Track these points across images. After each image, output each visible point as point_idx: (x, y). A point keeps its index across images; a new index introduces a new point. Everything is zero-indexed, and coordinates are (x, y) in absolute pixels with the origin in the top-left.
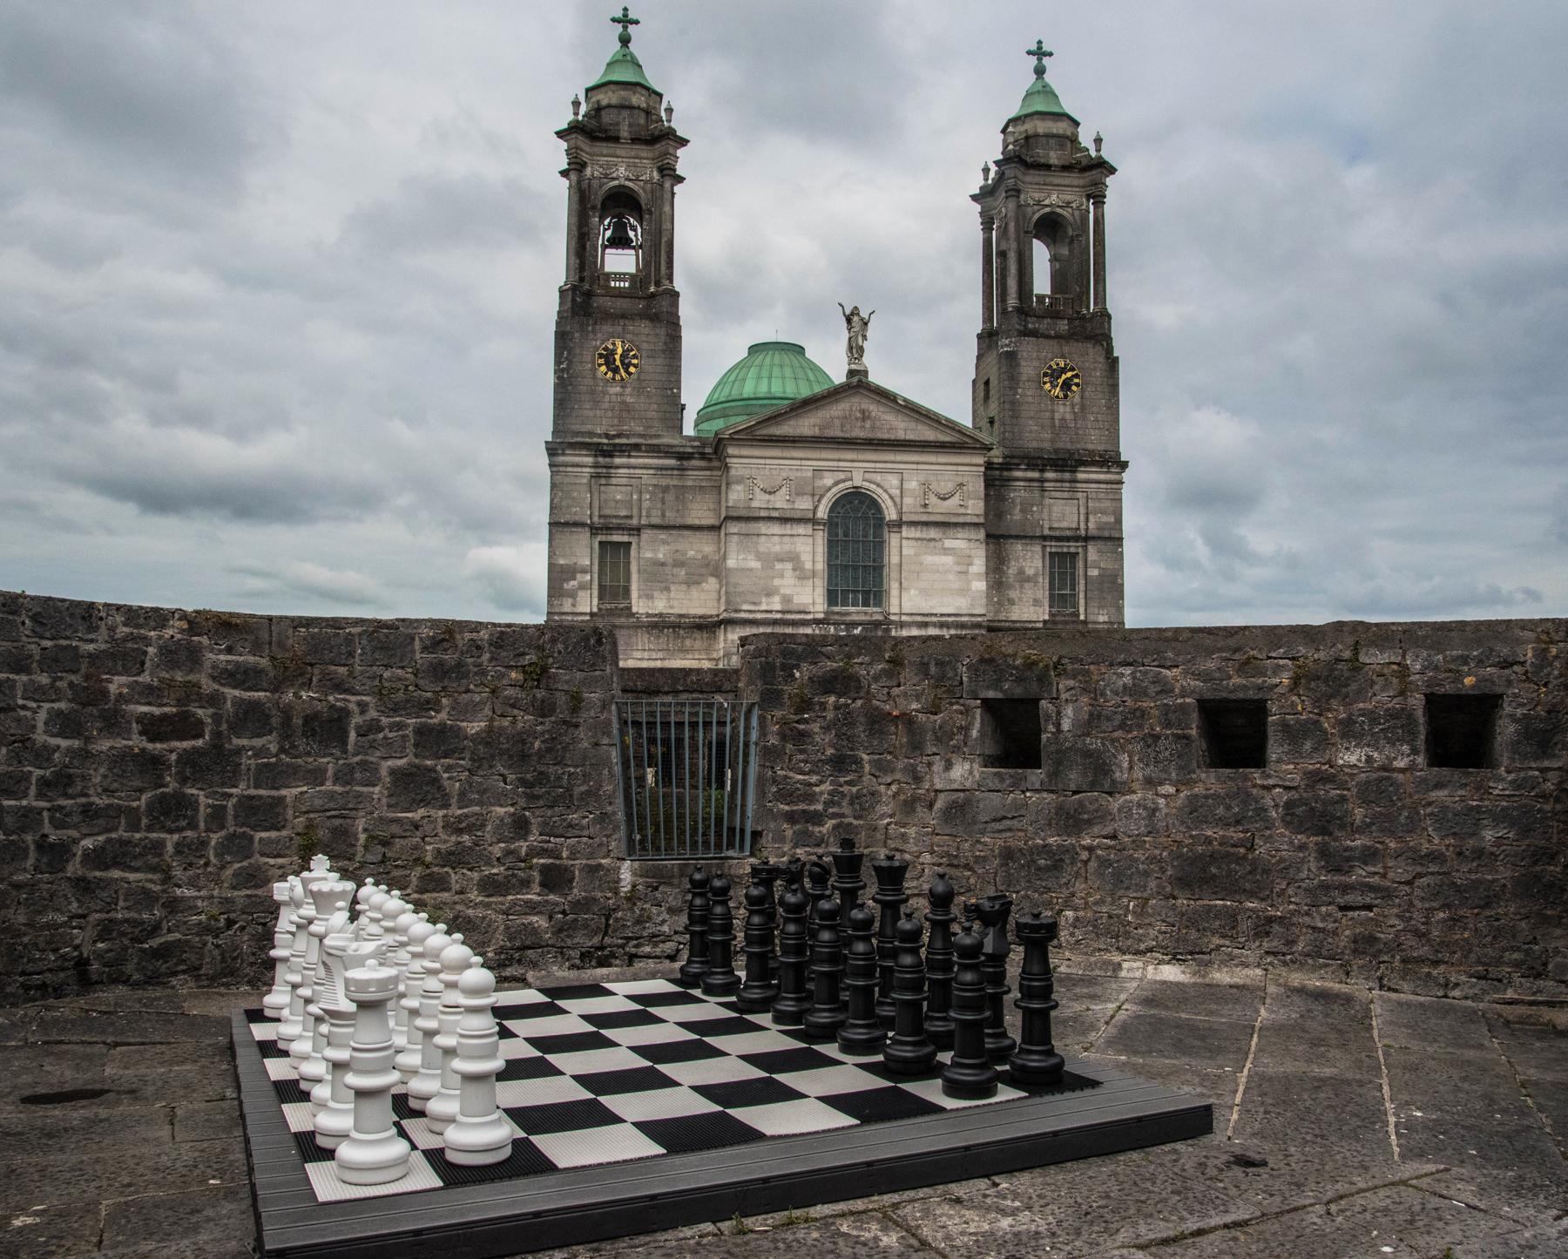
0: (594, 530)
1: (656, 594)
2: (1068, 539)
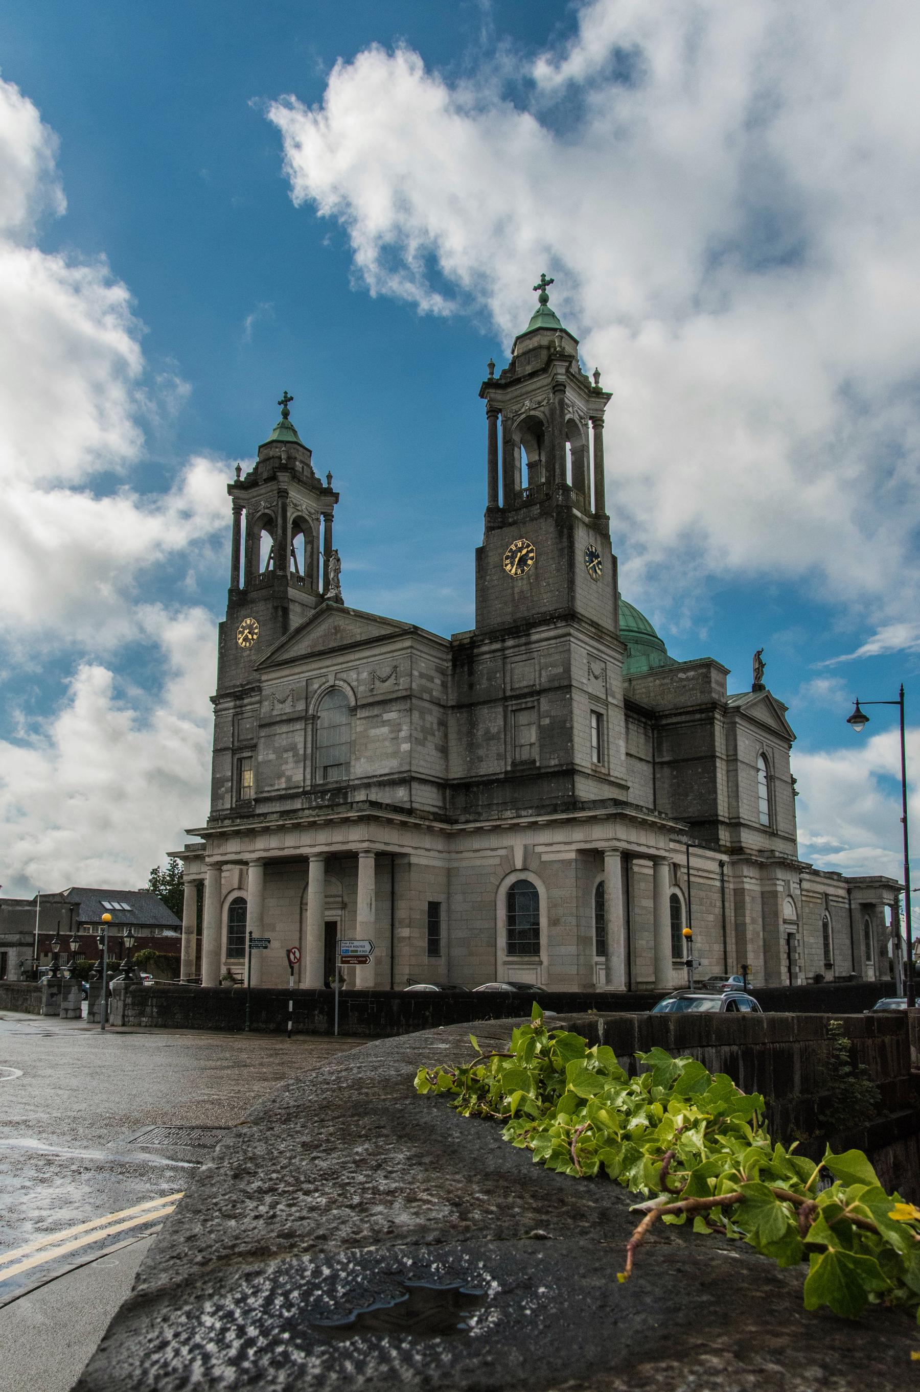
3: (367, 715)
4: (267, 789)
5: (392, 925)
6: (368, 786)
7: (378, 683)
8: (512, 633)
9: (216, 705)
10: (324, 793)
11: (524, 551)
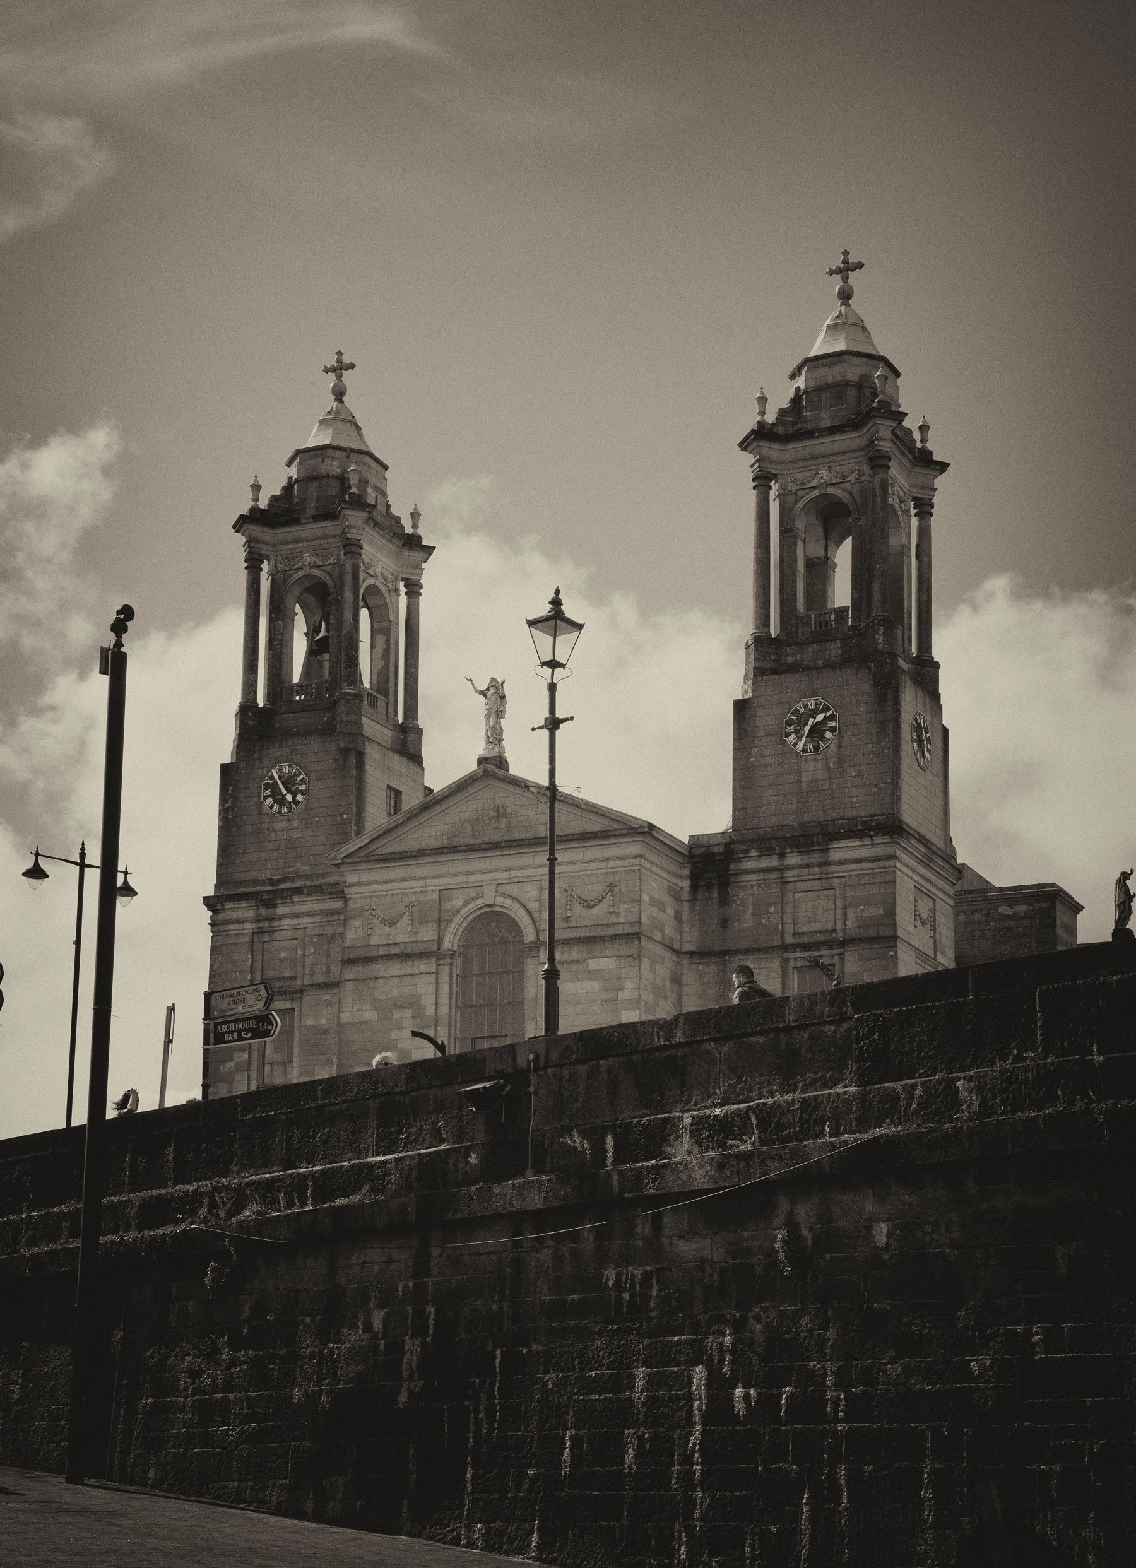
2: (818, 946)
7: (577, 908)
8: (797, 846)
9: (215, 912)
11: (820, 717)
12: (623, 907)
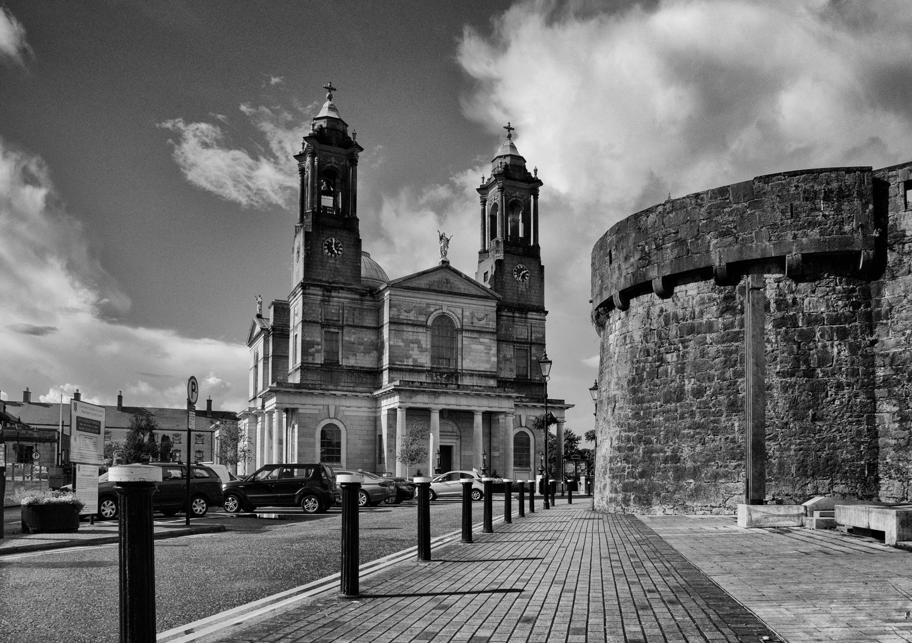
0: (323, 326)
1: (350, 357)
3: (469, 336)
4: (397, 363)
5: (490, 450)
6: (472, 375)
7: (475, 321)
10: (442, 374)
12: (491, 323)
